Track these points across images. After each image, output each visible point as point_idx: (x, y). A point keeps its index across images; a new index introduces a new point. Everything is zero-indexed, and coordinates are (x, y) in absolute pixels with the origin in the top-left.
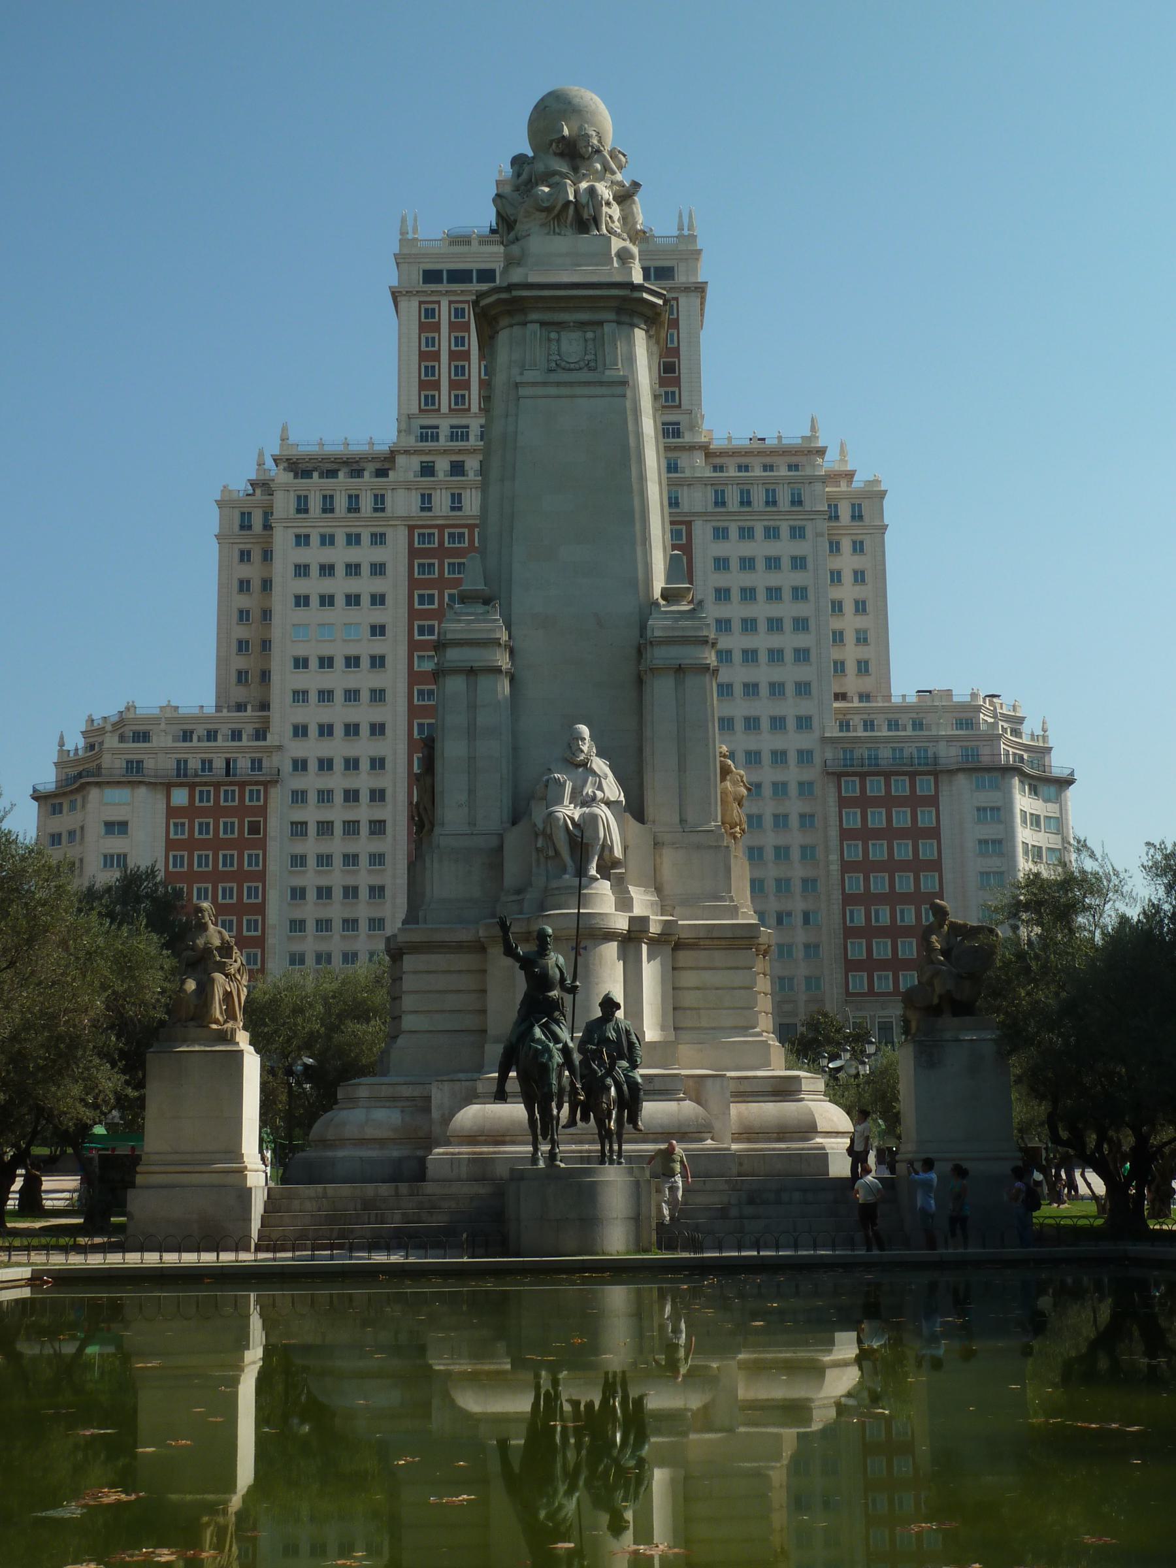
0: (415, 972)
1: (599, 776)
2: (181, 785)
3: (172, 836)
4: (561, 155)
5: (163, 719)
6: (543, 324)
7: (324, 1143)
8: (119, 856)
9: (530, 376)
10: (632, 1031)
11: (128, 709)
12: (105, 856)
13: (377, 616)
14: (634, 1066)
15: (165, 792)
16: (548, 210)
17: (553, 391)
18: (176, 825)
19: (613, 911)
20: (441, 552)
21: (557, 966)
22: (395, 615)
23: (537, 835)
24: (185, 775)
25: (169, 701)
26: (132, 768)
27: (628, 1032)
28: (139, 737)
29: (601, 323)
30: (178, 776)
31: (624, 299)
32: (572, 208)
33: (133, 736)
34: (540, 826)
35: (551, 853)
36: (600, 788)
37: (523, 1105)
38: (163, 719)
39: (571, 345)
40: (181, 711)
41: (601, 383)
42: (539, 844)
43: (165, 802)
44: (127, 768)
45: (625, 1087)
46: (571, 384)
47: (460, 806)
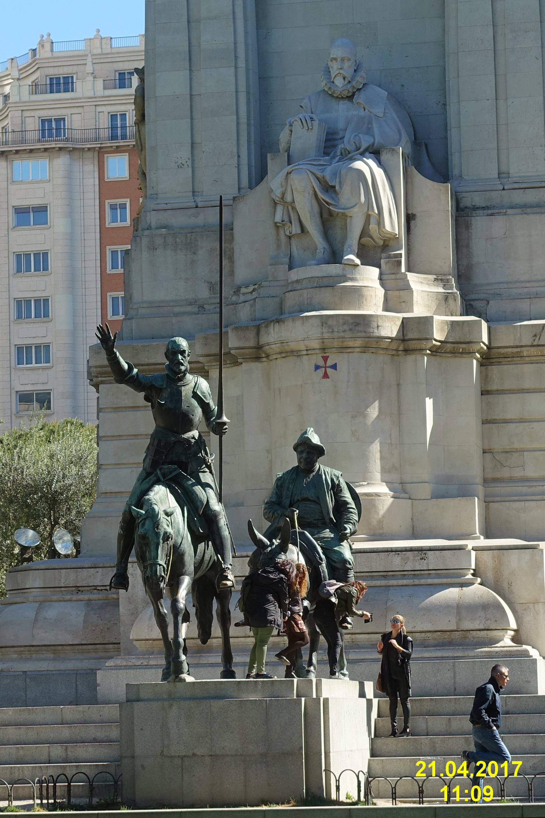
0: (117, 409)
2: (118, 150)
3: (108, 224)
5: (89, 59)
8: (36, 255)
10: (344, 486)
11: (42, 44)
12: (18, 256)
15: (96, 162)
18: (113, 207)
19: (379, 311)
21: (195, 396)
24: (124, 137)
25: (98, 31)
26: (50, 129)
27: (336, 489)
28: (58, 84)
30: (114, 137)
33: (51, 84)
35: (295, 229)
36: (369, 131)
38: (89, 59)
40: (115, 44)
42: (278, 218)
43: (97, 175)
44: (43, 130)
47: (181, 166)
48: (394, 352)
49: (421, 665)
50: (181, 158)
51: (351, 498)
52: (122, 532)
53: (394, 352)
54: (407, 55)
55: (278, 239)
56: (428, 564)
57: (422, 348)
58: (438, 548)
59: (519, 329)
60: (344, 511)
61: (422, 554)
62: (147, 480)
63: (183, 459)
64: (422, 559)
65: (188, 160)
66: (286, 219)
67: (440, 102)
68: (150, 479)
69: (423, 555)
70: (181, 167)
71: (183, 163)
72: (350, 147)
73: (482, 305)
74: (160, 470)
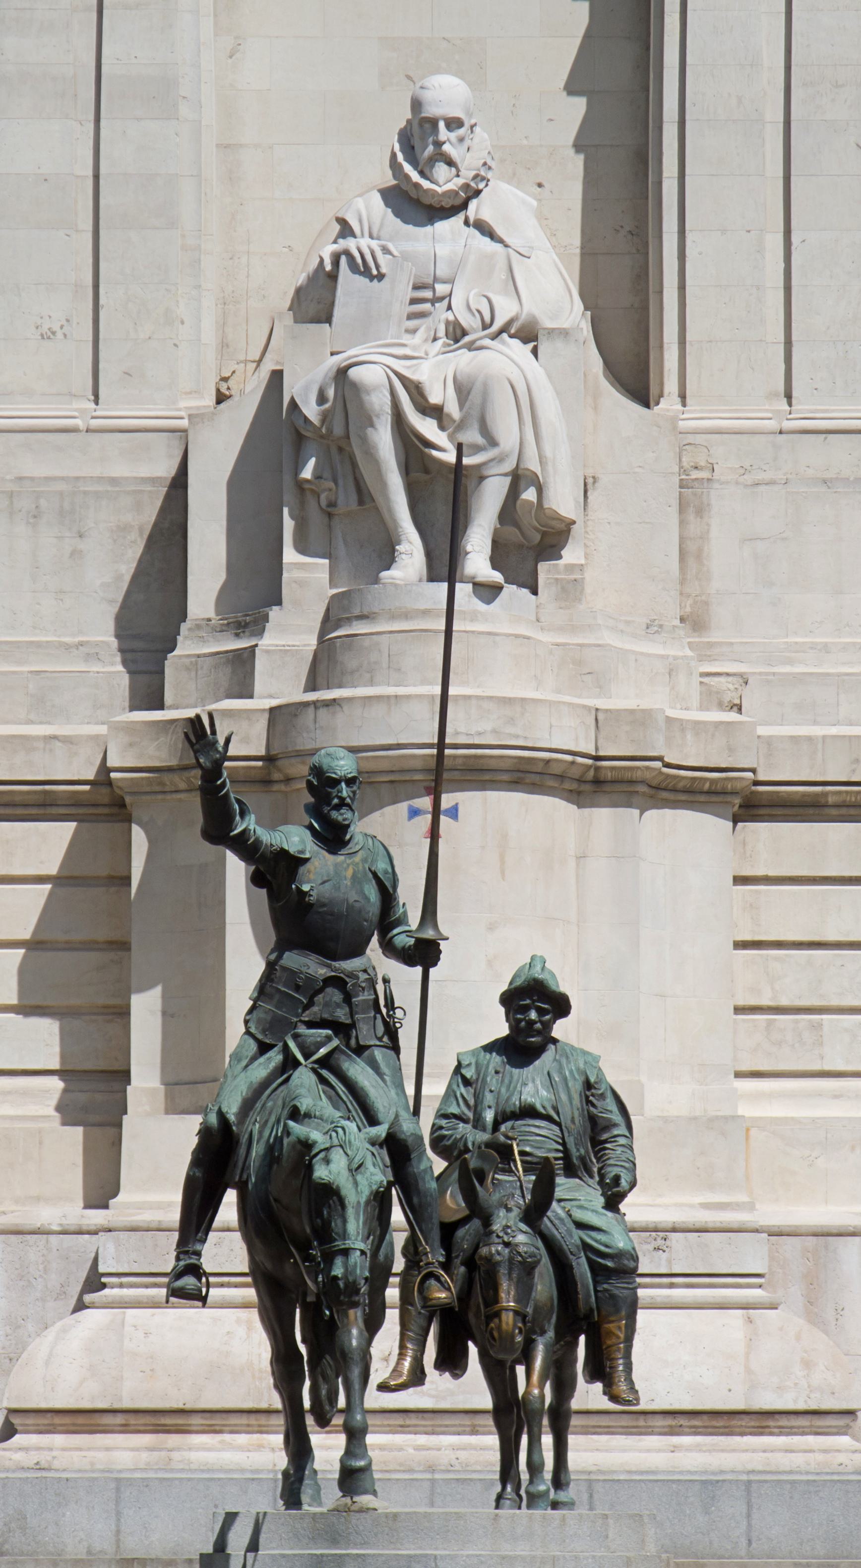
1: (506, 246)
14: (613, 1202)
23: (299, 440)
34: (311, 411)
37: (256, 1309)
45: (582, 1268)
47: (48, 336)
48: (574, 786)
49: (674, 1486)
50: (50, 317)
51: (618, 1112)
52: (198, 1174)
53: (574, 786)
54: (552, 117)
55: (302, 518)
56: (669, 1262)
57: (635, 780)
58: (691, 1226)
59: (820, 746)
60: (606, 1141)
61: (659, 1239)
62: (262, 1060)
63: (342, 1015)
64: (657, 1249)
65: (65, 323)
66: (327, 474)
67: (622, 227)
68: (269, 1059)
69: (660, 1242)
70: (49, 338)
71: (54, 329)
72: (467, 321)
73: (731, 687)
74: (296, 1037)
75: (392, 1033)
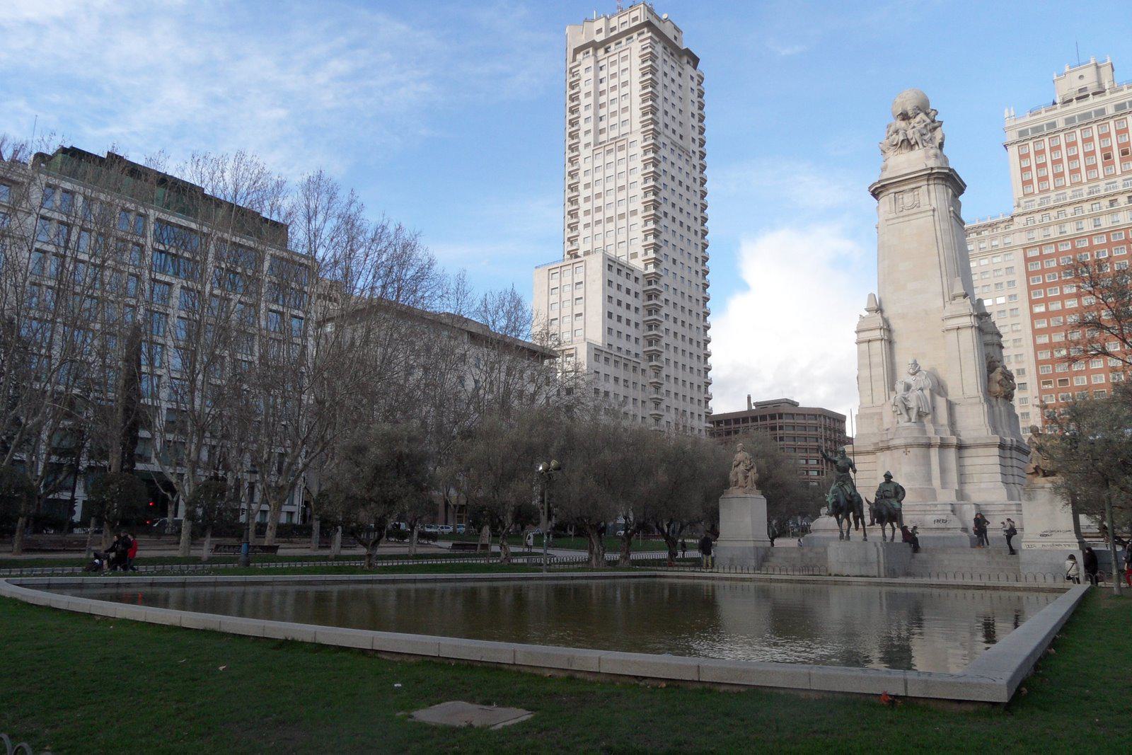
4: (903, 119)
6: (895, 193)
7: (816, 531)
9: (891, 216)
13: (1012, 292)
14: (899, 502)
16: (896, 145)
17: (901, 220)
20: (1042, 257)
22: (1021, 289)
29: (920, 187)
31: (930, 175)
32: (906, 143)
39: (908, 199)
41: (921, 212)
46: (909, 215)
75: (852, 482)
